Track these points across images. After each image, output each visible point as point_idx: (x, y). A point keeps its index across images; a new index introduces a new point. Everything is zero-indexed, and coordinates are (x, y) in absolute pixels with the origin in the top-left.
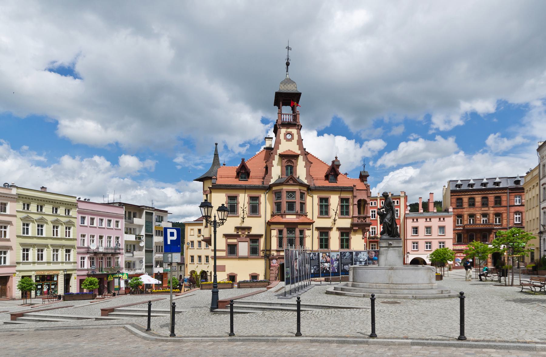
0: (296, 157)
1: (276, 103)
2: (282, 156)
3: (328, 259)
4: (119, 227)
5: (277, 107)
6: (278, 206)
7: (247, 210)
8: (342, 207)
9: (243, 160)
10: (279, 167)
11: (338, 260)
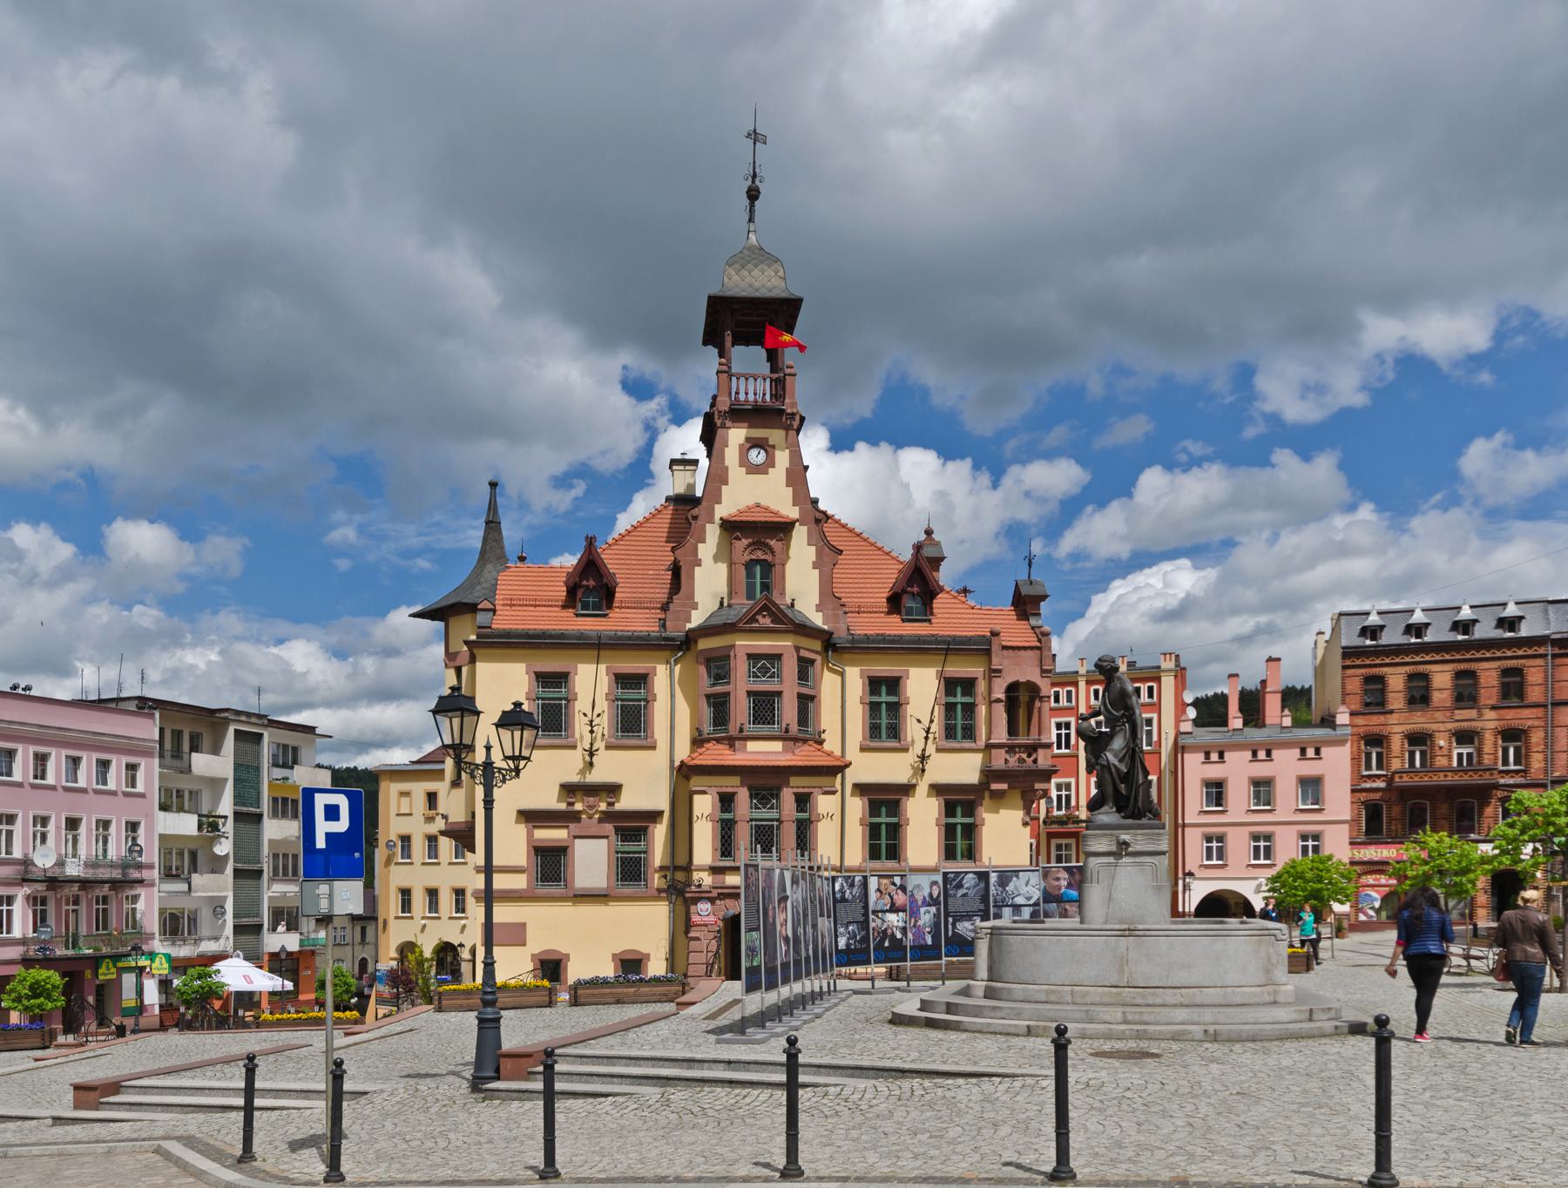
0: (783, 529)
1: (712, 337)
2: (731, 527)
3: (900, 899)
4: (140, 788)
5: (712, 351)
6: (720, 705)
7: (604, 724)
8: (950, 708)
9: (590, 541)
10: (723, 568)
11: (934, 901)
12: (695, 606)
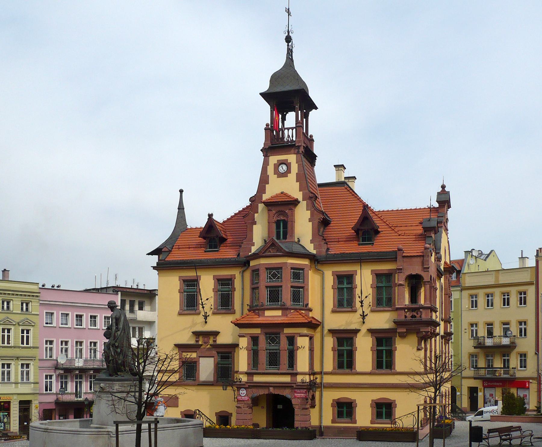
2: (269, 204)
12: (253, 244)
